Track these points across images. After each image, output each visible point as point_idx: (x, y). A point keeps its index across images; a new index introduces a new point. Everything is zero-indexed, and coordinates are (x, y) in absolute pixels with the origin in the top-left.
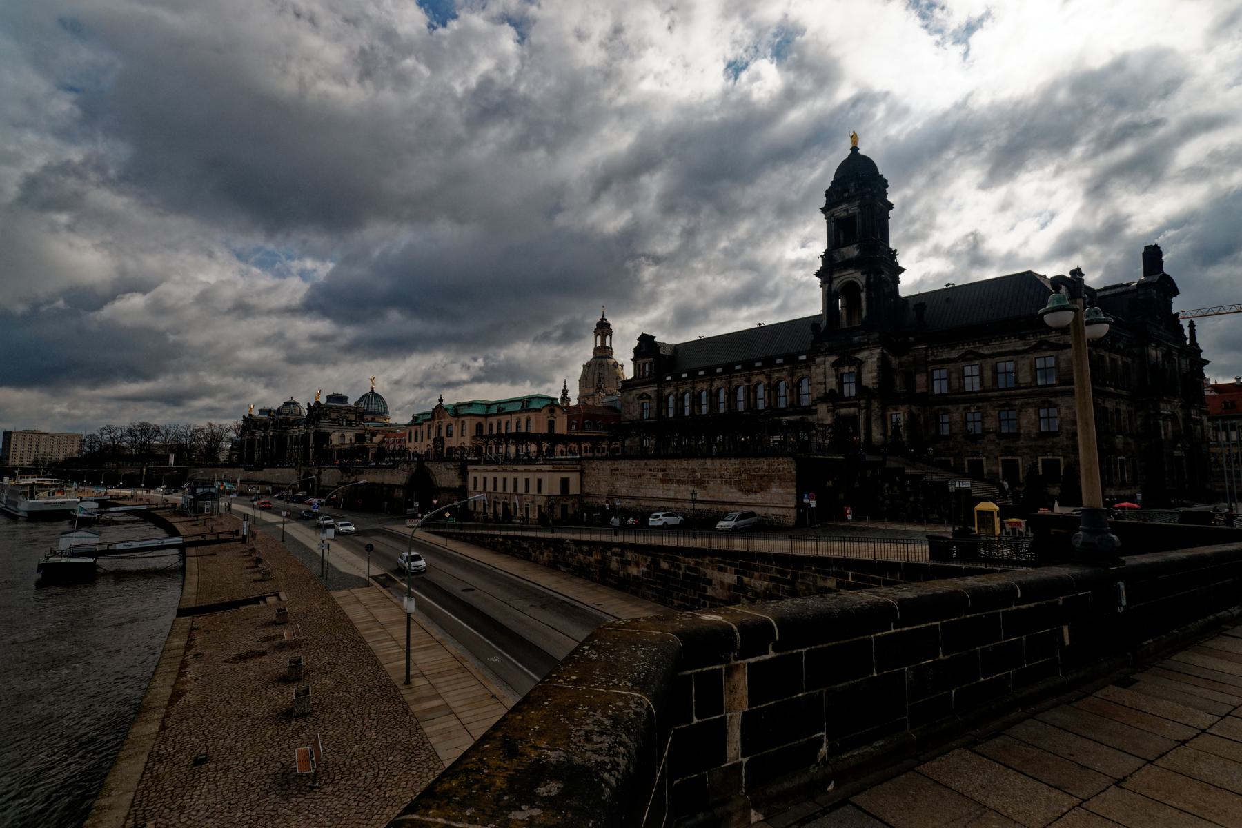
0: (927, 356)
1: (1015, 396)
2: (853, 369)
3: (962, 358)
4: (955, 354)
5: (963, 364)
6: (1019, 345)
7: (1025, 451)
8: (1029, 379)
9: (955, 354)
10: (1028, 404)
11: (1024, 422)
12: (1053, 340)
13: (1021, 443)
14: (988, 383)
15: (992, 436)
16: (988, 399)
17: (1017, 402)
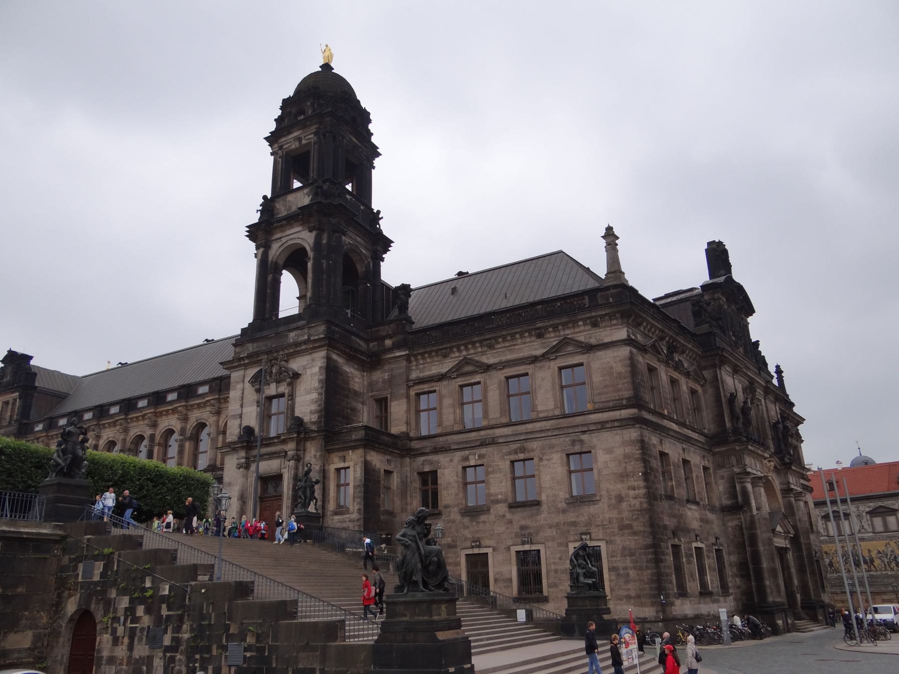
0: (409, 370)
1: (530, 436)
2: (283, 388)
3: (457, 371)
4: (445, 366)
5: (461, 381)
6: (536, 348)
7: (549, 533)
8: (551, 405)
9: (445, 366)
10: (552, 447)
11: (546, 479)
12: (581, 338)
13: (544, 517)
14: (495, 414)
15: (502, 508)
16: (493, 442)
17: (534, 445)
